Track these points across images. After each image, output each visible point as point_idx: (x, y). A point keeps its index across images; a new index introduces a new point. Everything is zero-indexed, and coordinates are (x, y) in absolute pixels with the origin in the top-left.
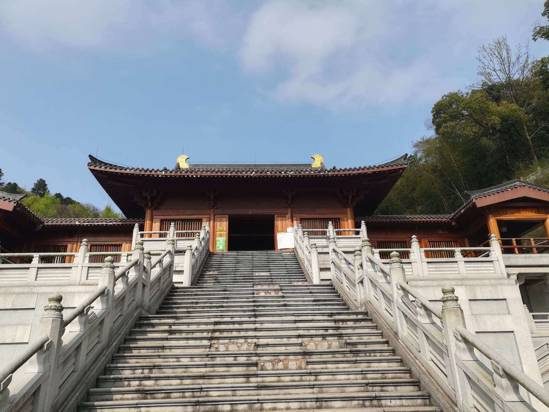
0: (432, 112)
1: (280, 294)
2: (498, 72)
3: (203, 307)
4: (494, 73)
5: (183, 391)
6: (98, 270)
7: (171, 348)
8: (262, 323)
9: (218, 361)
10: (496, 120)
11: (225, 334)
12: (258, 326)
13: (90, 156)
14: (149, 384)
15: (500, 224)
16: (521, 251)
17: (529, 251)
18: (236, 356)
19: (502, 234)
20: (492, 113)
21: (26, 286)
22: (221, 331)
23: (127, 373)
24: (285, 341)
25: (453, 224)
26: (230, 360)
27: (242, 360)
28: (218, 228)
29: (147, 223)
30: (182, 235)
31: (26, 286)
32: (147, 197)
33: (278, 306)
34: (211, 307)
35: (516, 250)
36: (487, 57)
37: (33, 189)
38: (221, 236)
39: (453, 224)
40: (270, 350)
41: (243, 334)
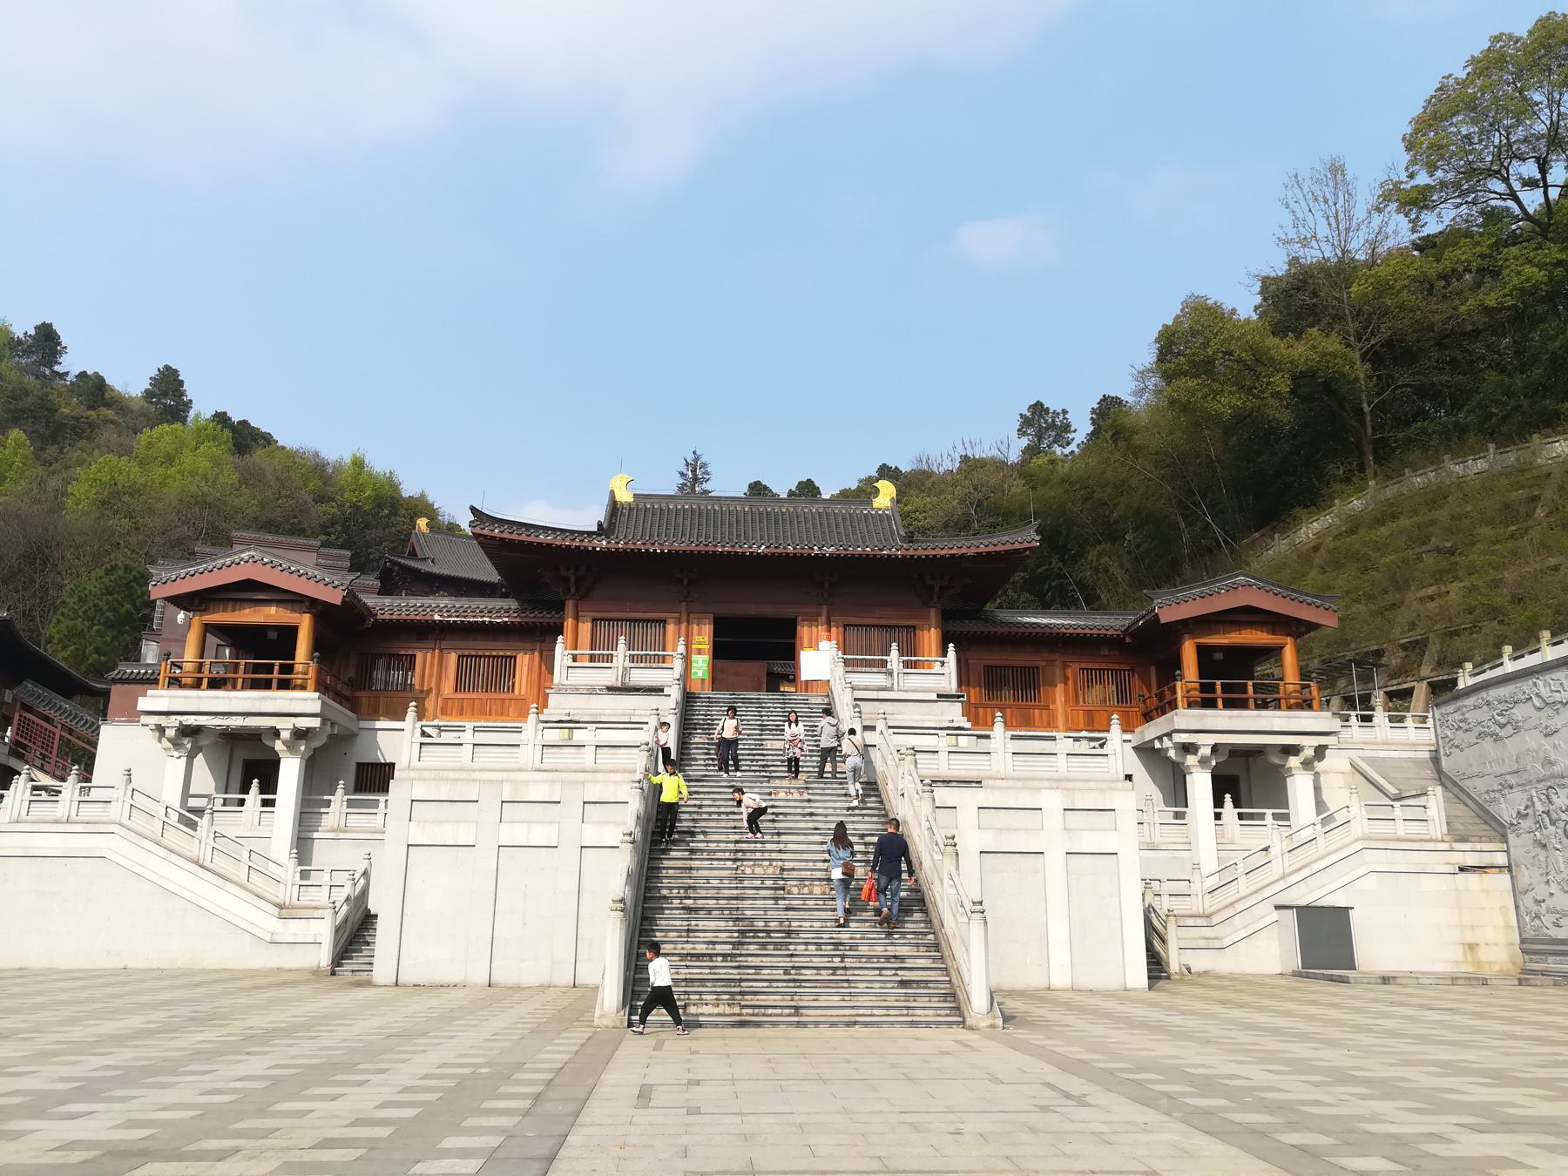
0: (1157, 340)
1: (806, 797)
2: (1323, 245)
3: (710, 813)
4: (1314, 243)
5: (722, 909)
6: (555, 750)
7: (698, 869)
8: (786, 843)
9: (746, 883)
10: (1282, 383)
11: (748, 855)
12: (781, 846)
13: (473, 509)
14: (689, 902)
15: (1203, 652)
16: (1230, 704)
17: (1241, 704)
18: (763, 880)
19: (1203, 673)
20: (1275, 365)
21: (461, 770)
22: (744, 851)
23: (665, 892)
24: (811, 865)
25: (1128, 640)
26: (757, 883)
27: (769, 883)
28: (697, 638)
29: (569, 624)
30: (641, 659)
31: (461, 770)
32: (567, 580)
33: (804, 815)
34: (719, 813)
35: (1220, 702)
36: (1303, 203)
37: (147, 391)
38: (699, 652)
39: (1128, 640)
40: (795, 874)
41: (766, 855)
